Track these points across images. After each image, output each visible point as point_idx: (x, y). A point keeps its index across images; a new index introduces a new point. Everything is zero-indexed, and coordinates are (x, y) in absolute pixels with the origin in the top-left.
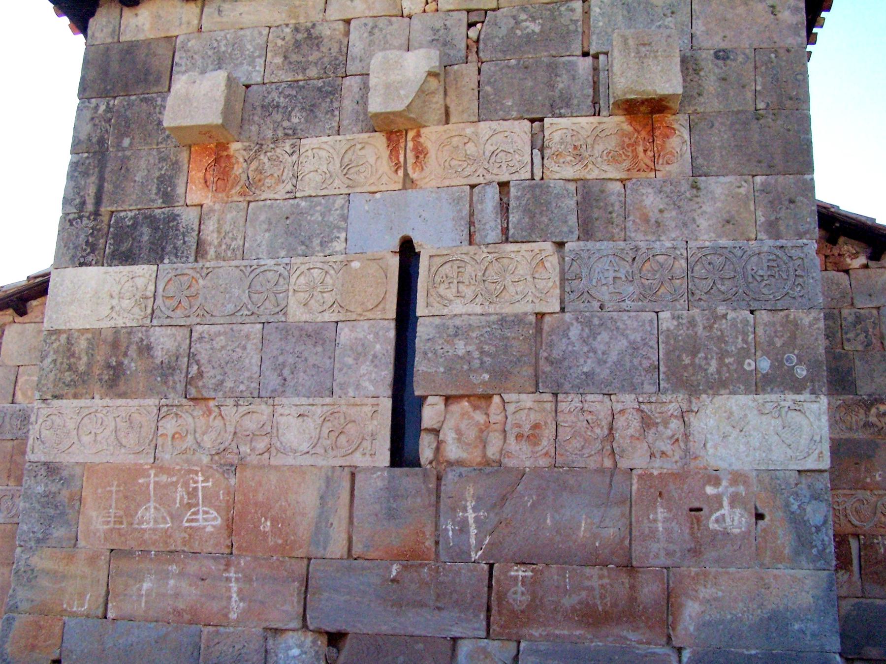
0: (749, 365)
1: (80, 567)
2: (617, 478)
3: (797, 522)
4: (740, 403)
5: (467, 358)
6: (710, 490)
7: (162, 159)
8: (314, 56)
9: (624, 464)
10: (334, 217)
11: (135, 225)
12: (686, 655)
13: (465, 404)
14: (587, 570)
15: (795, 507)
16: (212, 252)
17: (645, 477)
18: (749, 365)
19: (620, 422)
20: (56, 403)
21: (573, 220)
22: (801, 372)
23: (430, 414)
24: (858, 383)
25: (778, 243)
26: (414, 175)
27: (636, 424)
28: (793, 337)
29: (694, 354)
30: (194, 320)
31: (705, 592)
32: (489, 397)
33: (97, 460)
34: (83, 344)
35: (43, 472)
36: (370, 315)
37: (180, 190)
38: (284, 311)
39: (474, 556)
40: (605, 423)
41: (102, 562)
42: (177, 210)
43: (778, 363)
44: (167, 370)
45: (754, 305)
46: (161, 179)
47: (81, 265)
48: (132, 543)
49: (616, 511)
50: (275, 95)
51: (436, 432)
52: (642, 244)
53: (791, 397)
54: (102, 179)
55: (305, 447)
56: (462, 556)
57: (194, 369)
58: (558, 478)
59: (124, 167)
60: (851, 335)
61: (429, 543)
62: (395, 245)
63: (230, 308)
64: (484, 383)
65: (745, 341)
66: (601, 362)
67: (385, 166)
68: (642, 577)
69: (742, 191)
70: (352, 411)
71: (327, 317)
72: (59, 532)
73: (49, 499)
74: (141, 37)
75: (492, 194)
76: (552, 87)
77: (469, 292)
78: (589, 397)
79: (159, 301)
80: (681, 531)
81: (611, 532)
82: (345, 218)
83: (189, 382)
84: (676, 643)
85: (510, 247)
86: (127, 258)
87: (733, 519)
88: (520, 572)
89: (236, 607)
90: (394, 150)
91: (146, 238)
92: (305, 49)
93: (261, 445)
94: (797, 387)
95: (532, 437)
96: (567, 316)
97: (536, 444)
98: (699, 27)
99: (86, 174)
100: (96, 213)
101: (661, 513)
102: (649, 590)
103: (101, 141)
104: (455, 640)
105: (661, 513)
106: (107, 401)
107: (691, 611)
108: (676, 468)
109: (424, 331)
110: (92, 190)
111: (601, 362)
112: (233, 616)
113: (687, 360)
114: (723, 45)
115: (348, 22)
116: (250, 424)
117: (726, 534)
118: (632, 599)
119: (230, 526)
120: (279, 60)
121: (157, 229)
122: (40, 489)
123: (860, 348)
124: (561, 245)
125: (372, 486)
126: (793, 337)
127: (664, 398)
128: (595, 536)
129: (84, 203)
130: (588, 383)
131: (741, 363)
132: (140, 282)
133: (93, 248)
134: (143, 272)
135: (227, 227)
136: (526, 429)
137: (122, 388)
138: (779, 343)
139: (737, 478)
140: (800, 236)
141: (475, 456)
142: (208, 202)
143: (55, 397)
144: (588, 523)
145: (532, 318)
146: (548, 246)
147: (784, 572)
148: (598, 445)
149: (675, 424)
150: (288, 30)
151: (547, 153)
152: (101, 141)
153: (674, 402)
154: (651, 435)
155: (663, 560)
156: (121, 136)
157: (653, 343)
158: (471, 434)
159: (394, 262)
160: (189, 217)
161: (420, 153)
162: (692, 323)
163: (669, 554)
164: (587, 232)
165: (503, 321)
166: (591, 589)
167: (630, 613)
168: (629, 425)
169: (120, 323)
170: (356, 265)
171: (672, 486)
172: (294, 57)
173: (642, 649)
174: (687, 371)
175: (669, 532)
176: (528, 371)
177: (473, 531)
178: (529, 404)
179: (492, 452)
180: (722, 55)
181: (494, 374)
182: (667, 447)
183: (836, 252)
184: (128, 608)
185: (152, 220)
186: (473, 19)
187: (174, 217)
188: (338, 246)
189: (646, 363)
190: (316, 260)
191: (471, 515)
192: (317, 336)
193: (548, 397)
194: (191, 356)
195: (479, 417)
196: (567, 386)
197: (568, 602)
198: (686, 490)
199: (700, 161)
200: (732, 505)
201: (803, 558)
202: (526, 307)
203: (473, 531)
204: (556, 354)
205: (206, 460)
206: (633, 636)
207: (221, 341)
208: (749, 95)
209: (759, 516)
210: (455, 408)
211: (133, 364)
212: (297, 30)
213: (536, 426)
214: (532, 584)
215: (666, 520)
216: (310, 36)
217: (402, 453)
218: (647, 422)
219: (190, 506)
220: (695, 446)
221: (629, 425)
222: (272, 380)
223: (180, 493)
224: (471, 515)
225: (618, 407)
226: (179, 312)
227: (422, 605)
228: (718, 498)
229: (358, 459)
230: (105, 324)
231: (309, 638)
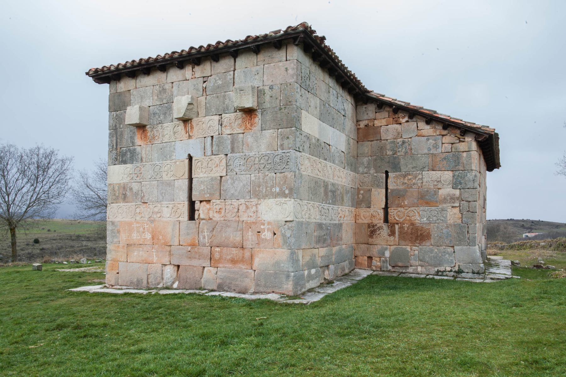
0: (274, 190)
2: (240, 223)
3: (284, 235)
4: (271, 201)
5: (203, 190)
6: (262, 227)
7: (131, 131)
8: (165, 95)
9: (241, 219)
11: (126, 152)
13: (205, 203)
14: (233, 249)
15: (283, 232)
16: (144, 160)
17: (247, 223)
18: (274, 190)
19: (241, 208)
21: (229, 147)
22: (287, 192)
23: (197, 205)
24: (402, 168)
25: (283, 151)
26: (191, 135)
27: (244, 208)
28: (285, 181)
29: (259, 187)
30: (141, 180)
31: (261, 255)
32: (210, 201)
33: (122, 220)
34: (117, 188)
36: (182, 178)
39: (207, 245)
40: (237, 208)
41: (125, 248)
42: (136, 147)
43: (281, 189)
44: (137, 194)
45: (276, 171)
46: (131, 137)
48: (131, 243)
49: (240, 233)
50: (156, 109)
52: (247, 154)
53: (284, 199)
54: (117, 138)
55: (168, 216)
56: (204, 245)
57: (142, 195)
58: (226, 223)
59: (122, 134)
60: (400, 150)
61: (197, 241)
63: (149, 176)
64: (208, 197)
65: (273, 183)
66: (236, 190)
67: (183, 132)
68: (246, 251)
69: (274, 135)
70: (179, 205)
71: (172, 178)
72: (116, 240)
76: (224, 103)
77: (204, 170)
78: (233, 201)
80: (255, 238)
81: (238, 239)
82: (174, 149)
84: (254, 269)
85: (214, 157)
86: (125, 162)
87: (267, 235)
88: (218, 249)
89: (155, 259)
90: (185, 127)
91: (129, 156)
92: (162, 93)
93: (159, 215)
94: (285, 196)
95: (219, 212)
96: (228, 177)
97: (221, 214)
98: (265, 78)
99: (113, 137)
100: (116, 149)
101: (250, 233)
102: (247, 254)
103: (116, 126)
104: (204, 267)
105: (250, 233)
106: (124, 204)
107: (257, 262)
108: (254, 221)
110: (115, 142)
111: (236, 190)
112: (154, 261)
113: (257, 189)
114: (272, 84)
115: (173, 83)
116: (156, 210)
117: (266, 239)
118: (243, 257)
119: (153, 238)
120: (156, 98)
121: (131, 153)
123: (403, 154)
124: (227, 155)
125: (183, 226)
126: (285, 181)
127: (252, 200)
128: (235, 240)
129: (113, 145)
130: (232, 197)
131: (271, 189)
132: (128, 169)
133: (116, 159)
134: (128, 165)
136: (218, 210)
137: (127, 200)
138: (282, 183)
139: (269, 223)
140: (289, 149)
141: (207, 217)
142: (142, 145)
145: (219, 178)
146: (223, 156)
147: (280, 250)
148: (234, 214)
149: (254, 208)
150: (158, 87)
151: (223, 126)
152: (116, 126)
153: (254, 201)
154: (248, 211)
155: (250, 247)
157: (249, 184)
158: (206, 211)
159: (187, 161)
160: (138, 149)
161: (192, 128)
162: (259, 178)
163: (252, 245)
164: (233, 151)
166: (233, 254)
167: (242, 260)
170: (178, 163)
171: (253, 226)
172: (160, 97)
173: (246, 271)
174: (257, 192)
175: (252, 238)
176: (218, 194)
177: (207, 238)
178: (219, 203)
179: (211, 216)
180: (271, 88)
181: (210, 194)
182: (252, 215)
183: (397, 116)
184: (132, 261)
185: (130, 150)
186: (205, 80)
188: (174, 157)
189: (247, 190)
190: (168, 162)
191: (206, 234)
192: (170, 184)
193: (223, 201)
194: (142, 191)
195: (208, 206)
196: (227, 198)
197: (229, 257)
198: (256, 227)
199: (263, 125)
200: (268, 230)
201: (285, 246)
203: (207, 238)
204: (225, 188)
205: (146, 219)
206: (243, 267)
207: (148, 186)
208: (278, 101)
209: (275, 234)
210: (202, 203)
211: (128, 193)
212: (160, 87)
213: (220, 209)
214: (220, 252)
215: (251, 235)
217: (192, 217)
218: (247, 207)
219: (144, 232)
220: (259, 215)
221: (242, 208)
223: (141, 229)
224: (206, 234)
225: (240, 203)
226: (138, 178)
227: (195, 258)
228: (264, 230)
229: (180, 219)
230: (122, 182)
231: (172, 267)
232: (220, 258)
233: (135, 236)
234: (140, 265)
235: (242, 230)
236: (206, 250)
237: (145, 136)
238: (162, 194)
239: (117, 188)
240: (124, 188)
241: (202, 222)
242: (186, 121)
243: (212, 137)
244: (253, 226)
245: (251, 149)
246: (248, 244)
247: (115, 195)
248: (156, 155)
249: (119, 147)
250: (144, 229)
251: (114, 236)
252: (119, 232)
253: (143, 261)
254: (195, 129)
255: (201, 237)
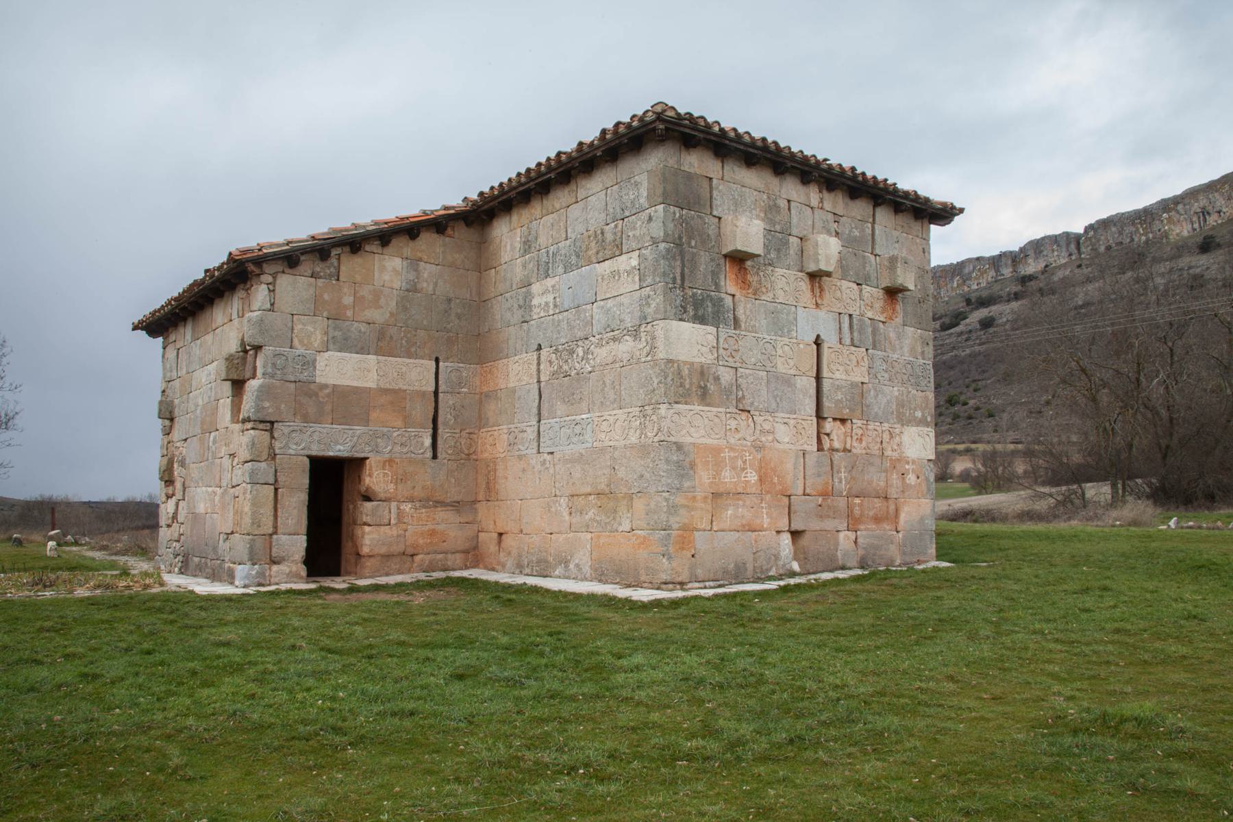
1: (700, 505)
3: (927, 479)
5: (840, 401)
7: (712, 260)
10: (791, 318)
11: (703, 300)
12: (900, 535)
20: (676, 406)
30: (738, 365)
31: (906, 509)
35: (674, 448)
37: (722, 283)
38: (775, 366)
42: (723, 295)
44: (728, 391)
46: (713, 272)
47: (681, 320)
48: (721, 490)
51: (828, 435)
54: (683, 266)
57: (740, 393)
62: (813, 338)
67: (808, 294)
68: (890, 502)
71: (793, 372)
72: (687, 484)
73: (679, 465)
74: (692, 170)
75: (847, 318)
79: (721, 351)
80: (900, 484)
82: (796, 319)
83: (738, 400)
88: (857, 501)
89: (766, 522)
93: (770, 438)
100: (682, 287)
101: (895, 476)
103: (680, 238)
105: (895, 476)
107: (903, 517)
109: (826, 384)
110: (678, 270)
116: (767, 426)
121: (714, 305)
122: (675, 458)
129: (674, 278)
135: (748, 313)
139: (914, 462)
142: (738, 296)
143: (676, 403)
144: (876, 479)
150: (765, 197)
152: (680, 238)
156: (690, 238)
160: (728, 301)
161: (822, 290)
165: (852, 384)
168: (886, 436)
169: (703, 360)
179: (848, 446)
184: (722, 526)
187: (721, 300)
192: (788, 381)
194: (738, 387)
197: (871, 513)
202: (859, 379)
211: (712, 387)
214: (861, 505)
216: (775, 205)
218: (891, 437)
219: (744, 469)
222: (774, 405)
223: (740, 462)
227: (828, 517)
229: (805, 447)
230: (697, 360)
232: (861, 515)
233: (727, 476)
234: (737, 534)
235: (886, 471)
236: (841, 503)
237: (744, 284)
238: (775, 397)
239: (686, 372)
240: (702, 373)
241: (837, 456)
242: (815, 277)
243: (850, 316)
244: (898, 466)
245: (894, 351)
246: (893, 493)
247: (682, 385)
248: (764, 322)
249: (687, 284)
250: (745, 462)
251: (682, 476)
252: (692, 466)
253: (743, 526)
254: (827, 295)
255: (836, 480)
